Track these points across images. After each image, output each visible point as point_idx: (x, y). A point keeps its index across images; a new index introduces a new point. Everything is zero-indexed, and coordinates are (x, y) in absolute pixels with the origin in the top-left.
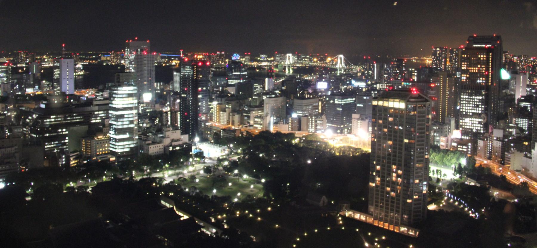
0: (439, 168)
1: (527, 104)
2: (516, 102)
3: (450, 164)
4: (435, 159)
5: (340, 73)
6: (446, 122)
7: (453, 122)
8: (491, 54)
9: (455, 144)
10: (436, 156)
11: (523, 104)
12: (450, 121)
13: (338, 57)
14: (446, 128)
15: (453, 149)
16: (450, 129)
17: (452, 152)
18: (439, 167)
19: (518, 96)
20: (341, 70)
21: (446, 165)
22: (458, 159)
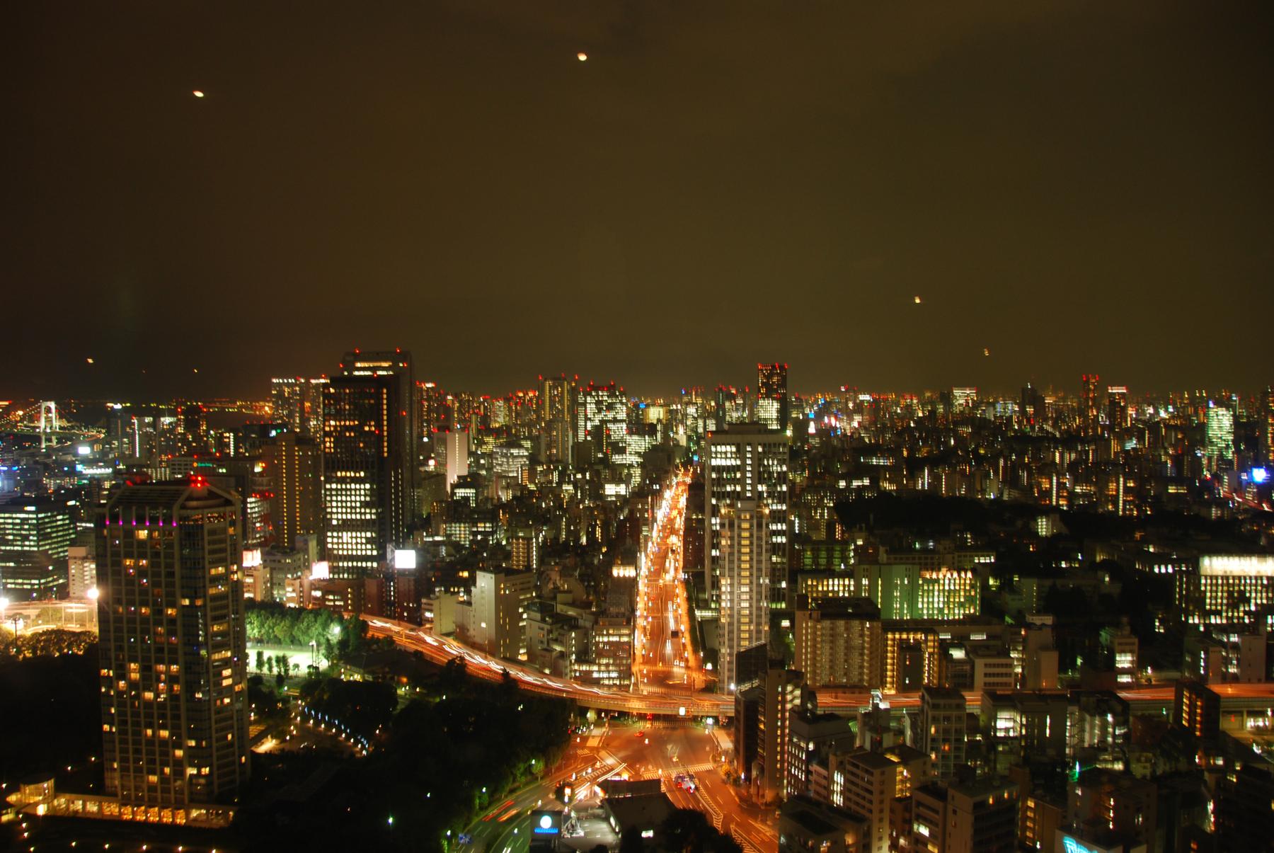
0: (281, 654)
1: (470, 492)
2: (449, 489)
3: (307, 639)
4: (274, 632)
5: (47, 447)
6: (299, 545)
7: (313, 545)
8: (385, 391)
9: (318, 594)
10: (275, 624)
11: (461, 492)
12: (306, 542)
13: (40, 407)
14: (300, 559)
15: (314, 604)
16: (307, 560)
17: (311, 611)
18: (284, 649)
19: (452, 478)
20: (49, 440)
21: (300, 644)
22: (325, 626)
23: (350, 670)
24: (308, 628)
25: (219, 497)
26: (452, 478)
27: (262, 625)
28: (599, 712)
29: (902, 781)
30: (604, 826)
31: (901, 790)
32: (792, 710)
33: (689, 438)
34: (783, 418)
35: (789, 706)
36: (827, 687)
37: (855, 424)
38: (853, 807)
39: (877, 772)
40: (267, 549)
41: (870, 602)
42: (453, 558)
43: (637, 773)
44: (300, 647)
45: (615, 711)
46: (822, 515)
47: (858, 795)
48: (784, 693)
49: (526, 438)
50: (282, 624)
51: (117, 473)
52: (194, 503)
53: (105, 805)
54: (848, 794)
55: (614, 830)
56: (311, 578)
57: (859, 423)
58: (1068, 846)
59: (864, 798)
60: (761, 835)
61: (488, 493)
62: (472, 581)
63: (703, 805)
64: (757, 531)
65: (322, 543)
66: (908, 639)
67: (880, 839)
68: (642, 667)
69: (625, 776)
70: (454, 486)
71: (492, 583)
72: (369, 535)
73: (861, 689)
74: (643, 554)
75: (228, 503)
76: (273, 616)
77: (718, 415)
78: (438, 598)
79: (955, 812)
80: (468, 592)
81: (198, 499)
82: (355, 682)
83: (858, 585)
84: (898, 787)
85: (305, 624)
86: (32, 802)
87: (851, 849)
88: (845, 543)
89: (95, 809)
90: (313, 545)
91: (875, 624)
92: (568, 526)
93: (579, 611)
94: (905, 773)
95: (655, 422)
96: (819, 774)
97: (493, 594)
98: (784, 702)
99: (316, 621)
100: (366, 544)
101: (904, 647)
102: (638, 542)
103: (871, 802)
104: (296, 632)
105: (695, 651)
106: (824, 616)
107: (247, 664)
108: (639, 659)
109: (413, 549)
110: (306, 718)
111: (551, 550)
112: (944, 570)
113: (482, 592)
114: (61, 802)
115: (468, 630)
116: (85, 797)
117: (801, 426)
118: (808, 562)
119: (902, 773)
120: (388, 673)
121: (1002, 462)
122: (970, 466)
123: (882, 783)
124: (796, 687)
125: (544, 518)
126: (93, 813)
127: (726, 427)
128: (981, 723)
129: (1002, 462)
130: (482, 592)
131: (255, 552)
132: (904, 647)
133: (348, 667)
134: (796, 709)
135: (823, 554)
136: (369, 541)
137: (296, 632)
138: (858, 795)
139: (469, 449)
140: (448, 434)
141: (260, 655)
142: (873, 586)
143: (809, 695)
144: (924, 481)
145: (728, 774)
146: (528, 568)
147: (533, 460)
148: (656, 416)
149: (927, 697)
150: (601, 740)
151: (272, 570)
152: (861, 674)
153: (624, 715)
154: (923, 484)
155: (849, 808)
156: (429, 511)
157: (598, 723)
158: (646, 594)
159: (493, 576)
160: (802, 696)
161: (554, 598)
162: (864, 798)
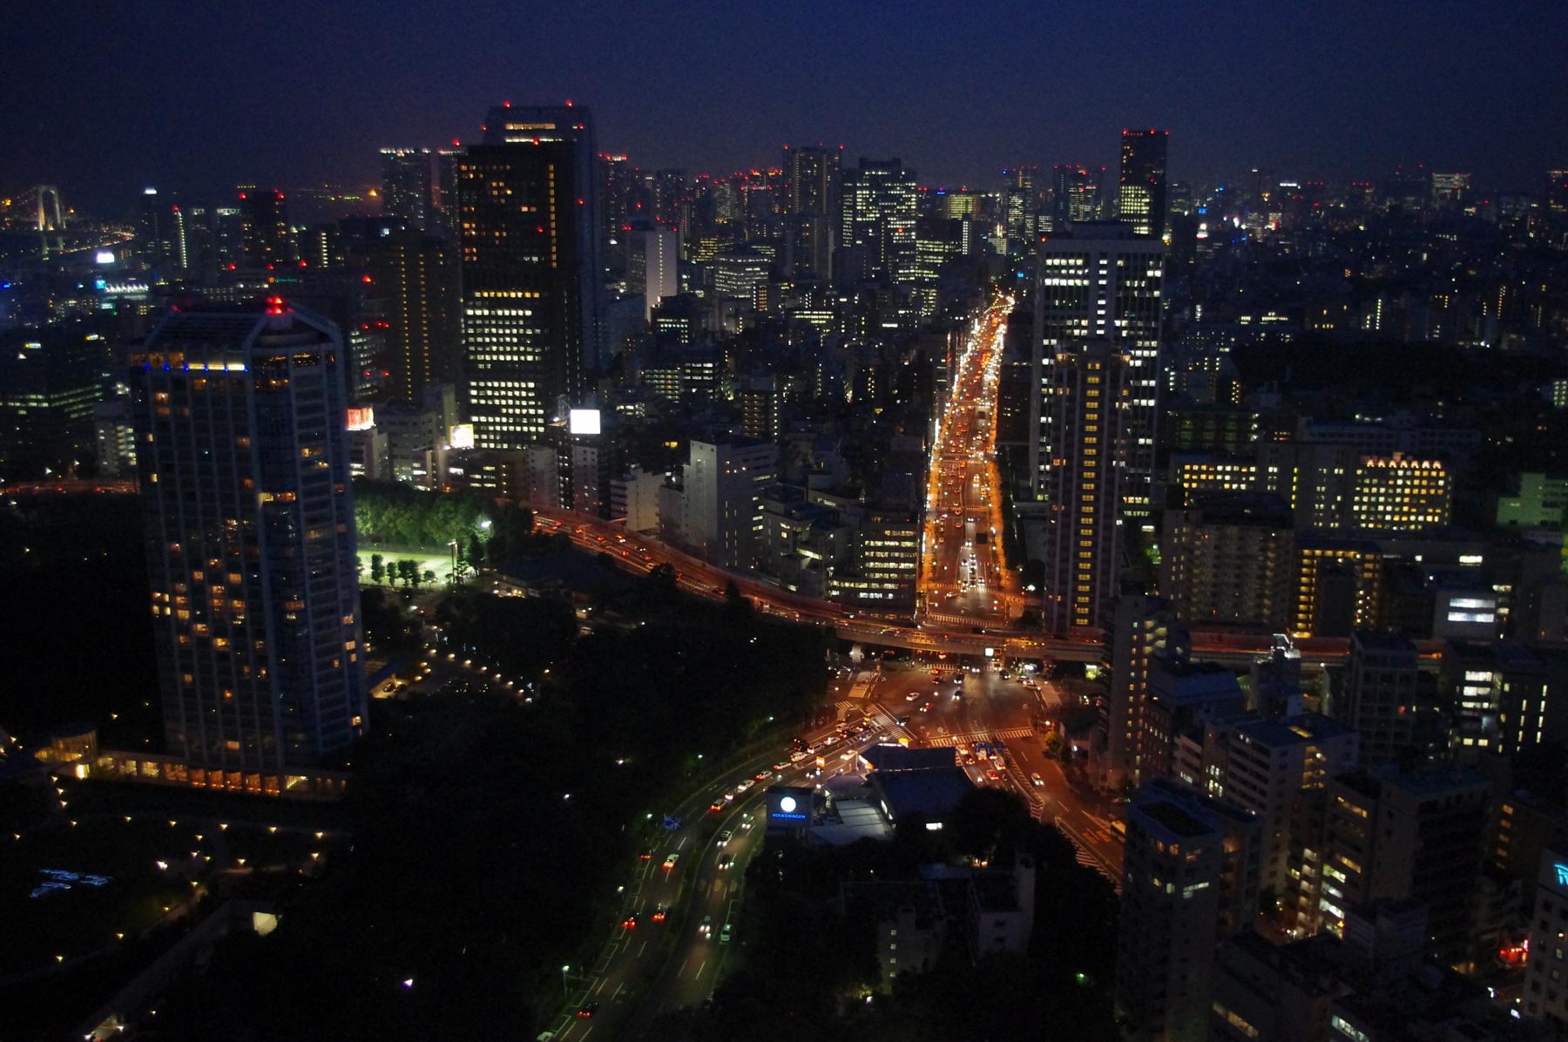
0: (407, 558)
2: (649, 317)
4: (395, 527)
5: (51, 254)
7: (449, 400)
8: (552, 168)
11: (666, 324)
12: (439, 396)
13: (36, 192)
14: (430, 421)
15: (452, 487)
17: (449, 497)
18: (410, 551)
20: (53, 243)
22: (470, 519)
23: (506, 582)
25: (309, 328)
26: (654, 300)
27: (378, 516)
28: (867, 649)
29: (1314, 767)
30: (872, 812)
31: (1311, 780)
32: (1151, 656)
33: (1012, 244)
34: (1157, 218)
35: (1148, 649)
36: (1207, 623)
37: (1272, 226)
38: (1237, 798)
39: (1275, 751)
40: (383, 405)
41: (1281, 498)
42: (656, 421)
43: (921, 735)
44: (432, 549)
47: (1245, 783)
48: (1142, 630)
49: (761, 241)
50: (407, 515)
51: (155, 292)
52: (272, 339)
53: (168, 767)
54: (1230, 780)
55: (885, 818)
57: (1277, 225)
58: (1560, 872)
59: (1254, 788)
60: (1100, 833)
61: (707, 323)
62: (683, 454)
63: (1016, 787)
65: (463, 396)
66: (1335, 558)
67: (1276, 848)
68: (932, 585)
70: (657, 313)
71: (713, 457)
73: (1261, 632)
74: (937, 421)
75: (323, 337)
76: (394, 504)
77: (1057, 208)
78: (634, 478)
79: (1390, 815)
80: (679, 472)
81: (280, 332)
82: (515, 598)
83: (1262, 473)
85: (441, 516)
86: (68, 760)
87: (1231, 860)
88: (1244, 410)
89: (154, 772)
90: (449, 400)
91: (1284, 533)
92: (825, 375)
93: (841, 501)
94: (1318, 755)
95: (960, 217)
96: (1189, 750)
97: (714, 473)
98: (1142, 643)
99: (456, 511)
101: (1327, 569)
102: (932, 400)
103: (1263, 793)
104: (428, 527)
105: (1011, 566)
106: (1208, 519)
107: (358, 573)
108: (927, 574)
109: (596, 408)
110: (444, 651)
111: (796, 410)
112: (1397, 456)
113: (699, 471)
114: (107, 761)
115: (678, 527)
116: (141, 755)
117: (1186, 228)
118: (1187, 435)
119: (1313, 755)
120: (562, 587)
121: (1503, 291)
122: (1452, 295)
123: (1283, 767)
124: (1160, 623)
125: (791, 363)
126: (151, 777)
127: (1069, 227)
128: (1440, 688)
129: (1503, 291)
130: (699, 471)
131: (365, 410)
133: (505, 578)
134: (1159, 654)
135: (1211, 425)
137: (428, 527)
138: (1245, 783)
139: (678, 258)
140: (648, 235)
141: (376, 560)
142: (1285, 475)
143: (1180, 634)
144: (1373, 320)
145: (1054, 744)
146: (766, 436)
147: (775, 273)
148: (962, 208)
149: (1358, 645)
150: (869, 689)
151: (391, 435)
152: (1260, 606)
153: (905, 653)
154: (1373, 321)
155: (1231, 801)
156: (620, 349)
157: (866, 664)
158: (940, 478)
159: (715, 447)
160: (1167, 637)
161: (804, 482)
162: (1254, 788)
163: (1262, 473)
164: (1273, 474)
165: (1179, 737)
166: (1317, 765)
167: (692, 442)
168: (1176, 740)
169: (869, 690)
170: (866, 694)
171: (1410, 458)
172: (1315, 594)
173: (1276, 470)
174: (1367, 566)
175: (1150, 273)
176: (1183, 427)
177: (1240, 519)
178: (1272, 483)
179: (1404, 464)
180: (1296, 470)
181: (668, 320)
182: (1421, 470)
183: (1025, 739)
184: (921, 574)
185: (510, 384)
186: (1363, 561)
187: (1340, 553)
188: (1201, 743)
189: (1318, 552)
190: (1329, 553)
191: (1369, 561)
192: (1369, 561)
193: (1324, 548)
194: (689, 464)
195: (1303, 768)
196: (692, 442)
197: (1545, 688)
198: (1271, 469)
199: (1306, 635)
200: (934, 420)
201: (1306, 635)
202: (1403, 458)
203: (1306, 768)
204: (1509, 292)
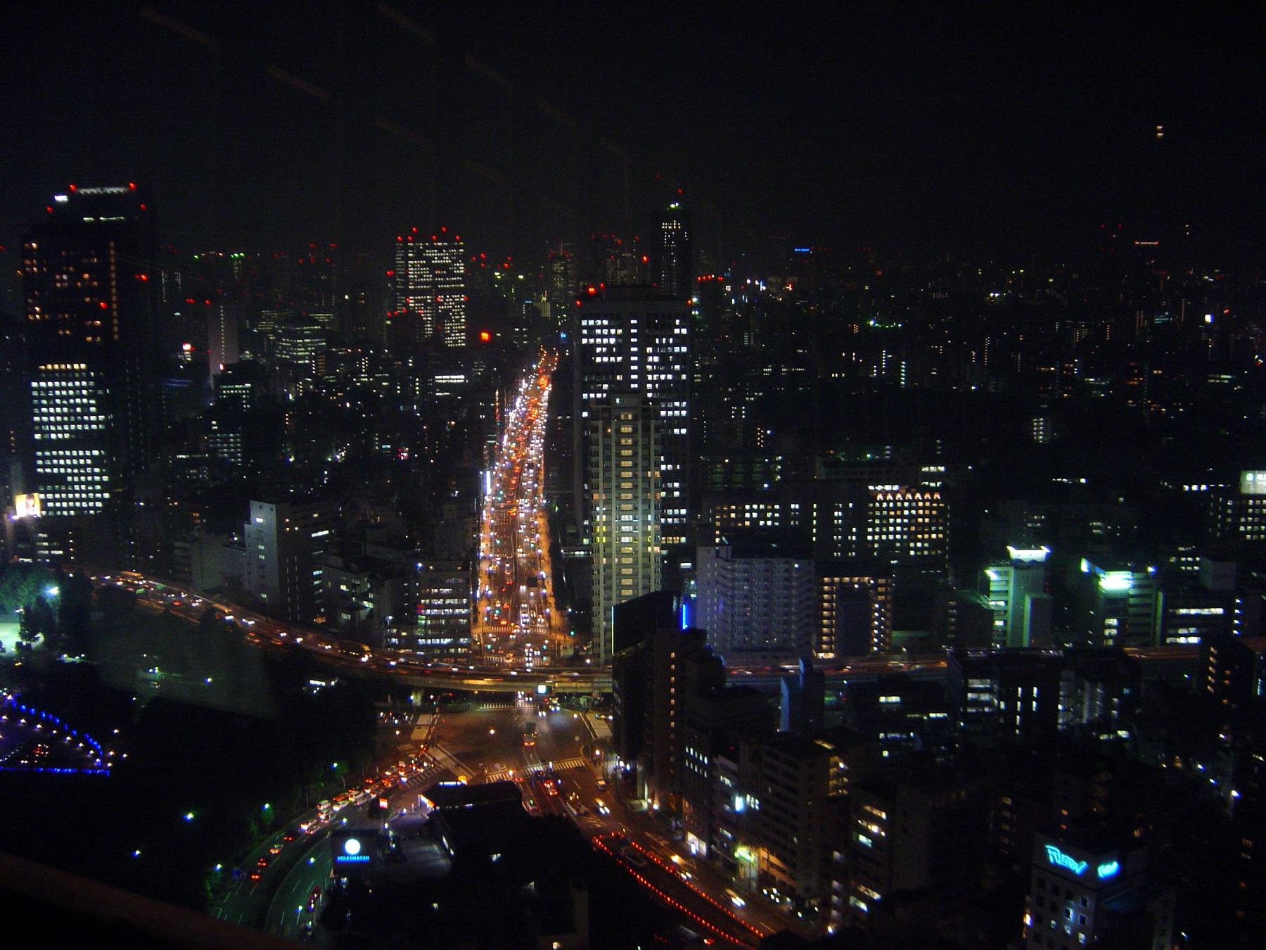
24: (14, 588)
28: (427, 692)
31: (836, 788)
45: (448, 691)
46: (738, 413)
56: (15, 518)
58: (1050, 852)
64: (643, 437)
65: (30, 465)
66: (852, 583)
68: (487, 629)
69: (463, 780)
71: (273, 516)
72: (96, 453)
74: (488, 473)
80: (241, 533)
84: (832, 783)
94: (842, 765)
97: (274, 531)
100: (92, 466)
101: (844, 592)
121: (988, 342)
129: (988, 342)
132: (844, 592)
136: (97, 462)
142: (805, 512)
157: (426, 708)
159: (273, 506)
163: (785, 511)
164: (795, 510)
165: (717, 757)
166: (842, 773)
167: (252, 502)
168: (715, 760)
169: (429, 732)
170: (428, 735)
171: (913, 490)
172: (836, 618)
173: (797, 506)
174: (880, 589)
175: (677, 331)
176: (714, 471)
177: (765, 553)
178: (795, 518)
179: (909, 496)
180: (815, 506)
181: (229, 387)
182: (924, 501)
183: (578, 769)
184: (476, 620)
185: (75, 453)
186: (876, 586)
187: (856, 579)
188: (735, 760)
189: (836, 579)
190: (847, 579)
191: (881, 585)
192: (881, 585)
193: (842, 576)
194: (250, 524)
195: (829, 778)
196: (252, 502)
197: (1035, 690)
198: (793, 506)
199: (831, 655)
200: (485, 472)
201: (831, 655)
202: (908, 491)
203: (831, 778)
204: (992, 341)
